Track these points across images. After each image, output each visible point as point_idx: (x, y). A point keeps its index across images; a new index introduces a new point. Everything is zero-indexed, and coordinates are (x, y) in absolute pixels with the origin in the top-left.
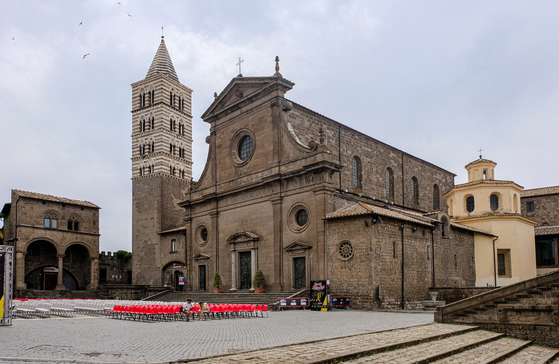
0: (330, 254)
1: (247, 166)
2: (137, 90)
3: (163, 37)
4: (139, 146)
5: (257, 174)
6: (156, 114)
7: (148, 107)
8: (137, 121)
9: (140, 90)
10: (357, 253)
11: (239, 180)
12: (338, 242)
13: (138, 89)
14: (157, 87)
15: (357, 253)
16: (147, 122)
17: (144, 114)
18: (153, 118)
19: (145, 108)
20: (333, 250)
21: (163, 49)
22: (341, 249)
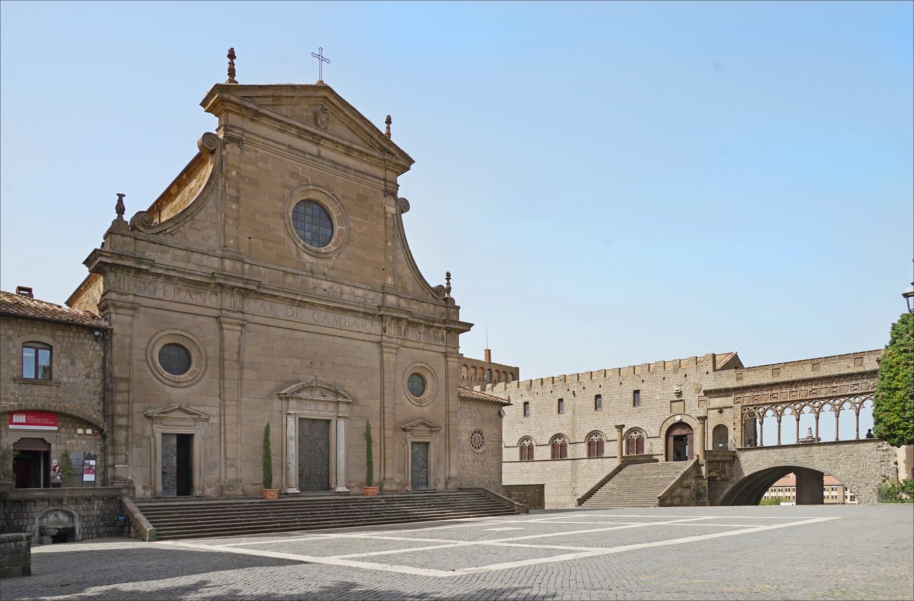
0: (462, 443)
1: (330, 263)
5: (355, 289)
10: (489, 445)
11: (311, 280)
12: (473, 429)
15: (489, 445)
20: (465, 438)
22: (472, 438)
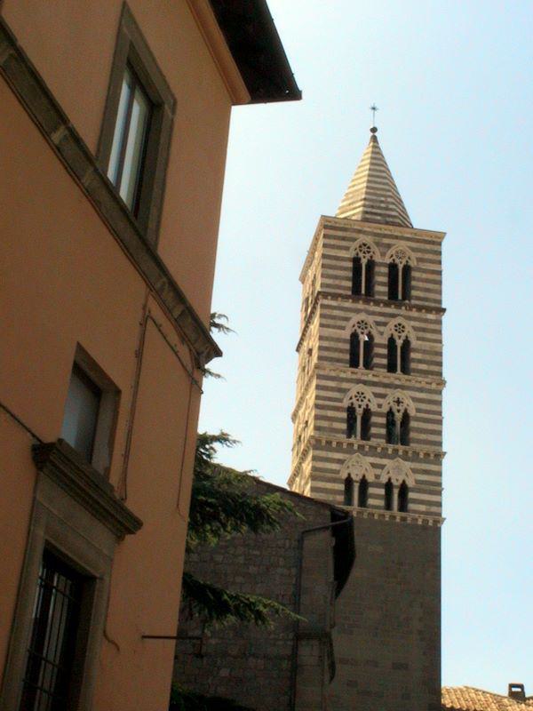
2: (343, 239)
3: (374, 130)
4: (346, 406)
6: (421, 334)
7: (387, 305)
8: (343, 328)
9: (356, 244)
13: (354, 240)
14: (419, 260)
16: (380, 346)
17: (370, 319)
18: (407, 343)
19: (377, 303)
21: (377, 161)
